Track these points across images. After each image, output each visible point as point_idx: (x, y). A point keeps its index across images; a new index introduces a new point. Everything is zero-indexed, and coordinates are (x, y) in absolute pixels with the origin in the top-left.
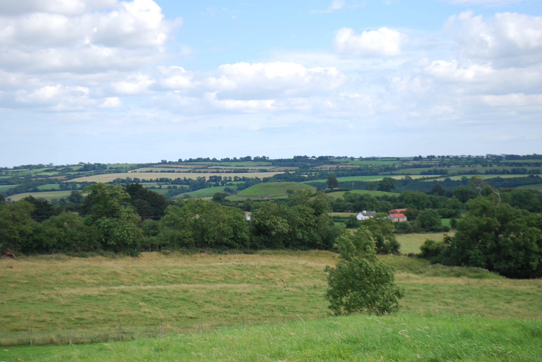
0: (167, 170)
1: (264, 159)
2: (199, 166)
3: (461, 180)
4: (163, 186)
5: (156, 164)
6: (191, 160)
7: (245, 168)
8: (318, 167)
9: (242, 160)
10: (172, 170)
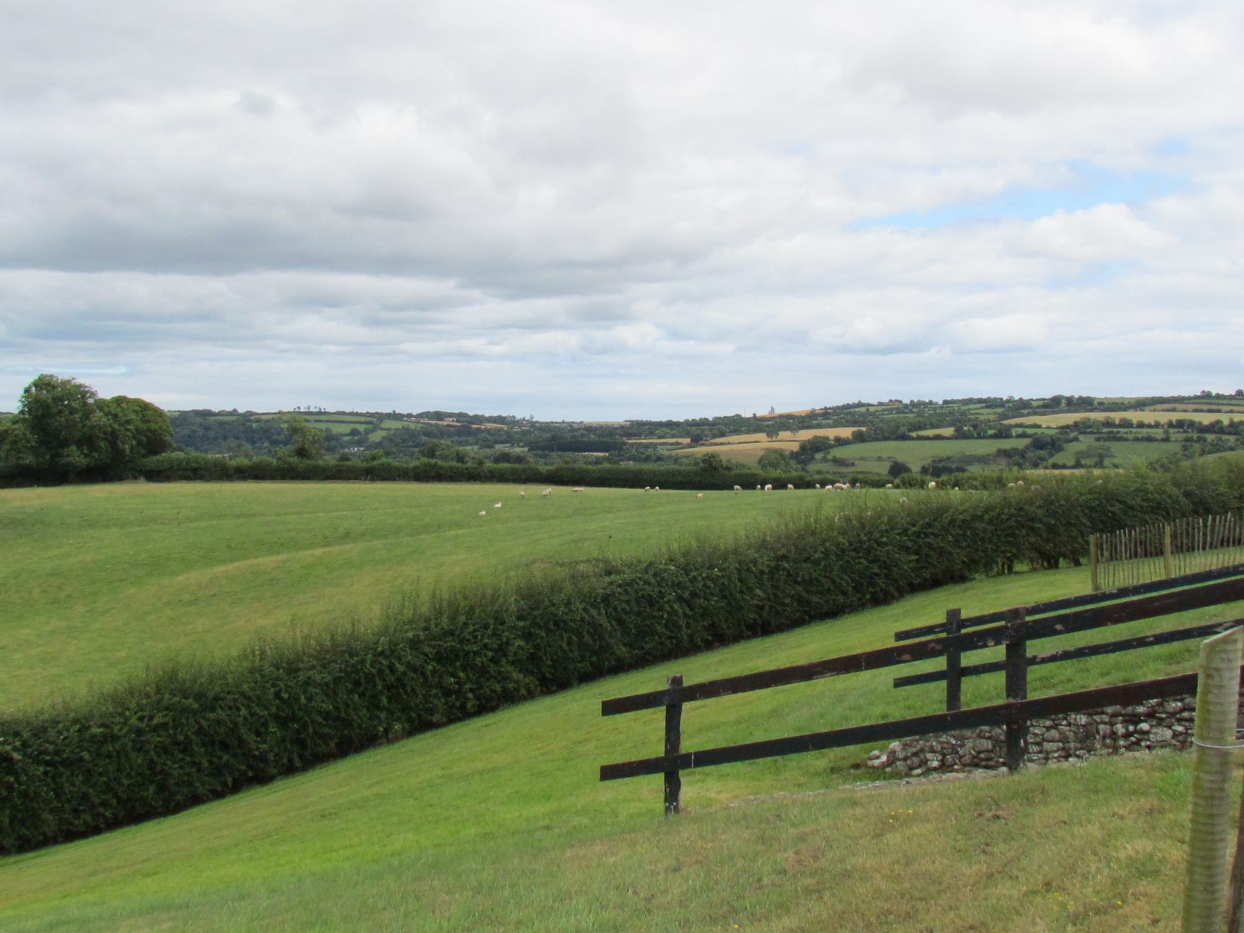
0: (1205, 407)
4: (1173, 437)
5: (1189, 398)
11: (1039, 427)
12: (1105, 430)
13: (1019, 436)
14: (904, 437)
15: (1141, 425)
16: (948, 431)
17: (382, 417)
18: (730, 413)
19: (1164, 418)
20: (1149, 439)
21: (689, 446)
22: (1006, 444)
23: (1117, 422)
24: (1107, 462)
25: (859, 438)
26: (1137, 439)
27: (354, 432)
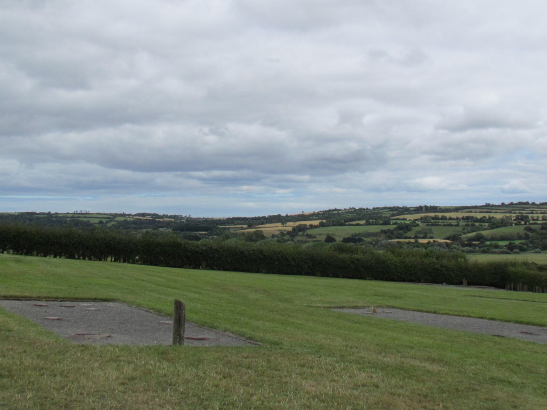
2: (514, 208)
5: (480, 207)
6: (512, 204)
10: (489, 210)
11: (406, 219)
13: (394, 224)
14: (342, 225)
15: (451, 219)
17: (116, 215)
18: (276, 214)
19: (460, 215)
20: (450, 225)
21: (246, 229)
22: (385, 228)
23: (440, 217)
24: (429, 235)
25: (322, 225)
26: (445, 225)
27: (101, 222)
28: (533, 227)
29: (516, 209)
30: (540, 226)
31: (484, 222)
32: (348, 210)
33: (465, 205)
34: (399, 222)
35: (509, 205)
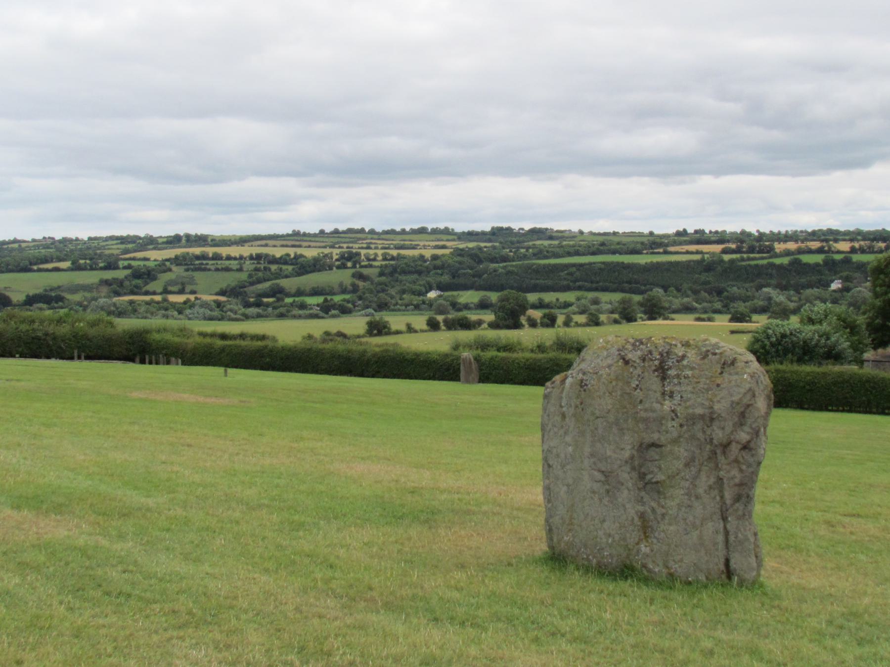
1: (447, 231)
3: (821, 263)
4: (245, 267)
5: (282, 236)
6: (336, 232)
7: (414, 243)
8: (531, 243)
9: (414, 232)
10: (297, 243)
12: (197, 262)
13: (125, 268)
15: (229, 258)
16: (66, 265)
19: (246, 251)
20: (227, 269)
22: (109, 275)
23: (211, 255)
24: (188, 288)
26: (217, 270)
28: (365, 271)
29: (340, 240)
30: (377, 271)
31: (286, 263)
32: (39, 241)
33: (257, 233)
34: (133, 263)
35: (332, 233)
